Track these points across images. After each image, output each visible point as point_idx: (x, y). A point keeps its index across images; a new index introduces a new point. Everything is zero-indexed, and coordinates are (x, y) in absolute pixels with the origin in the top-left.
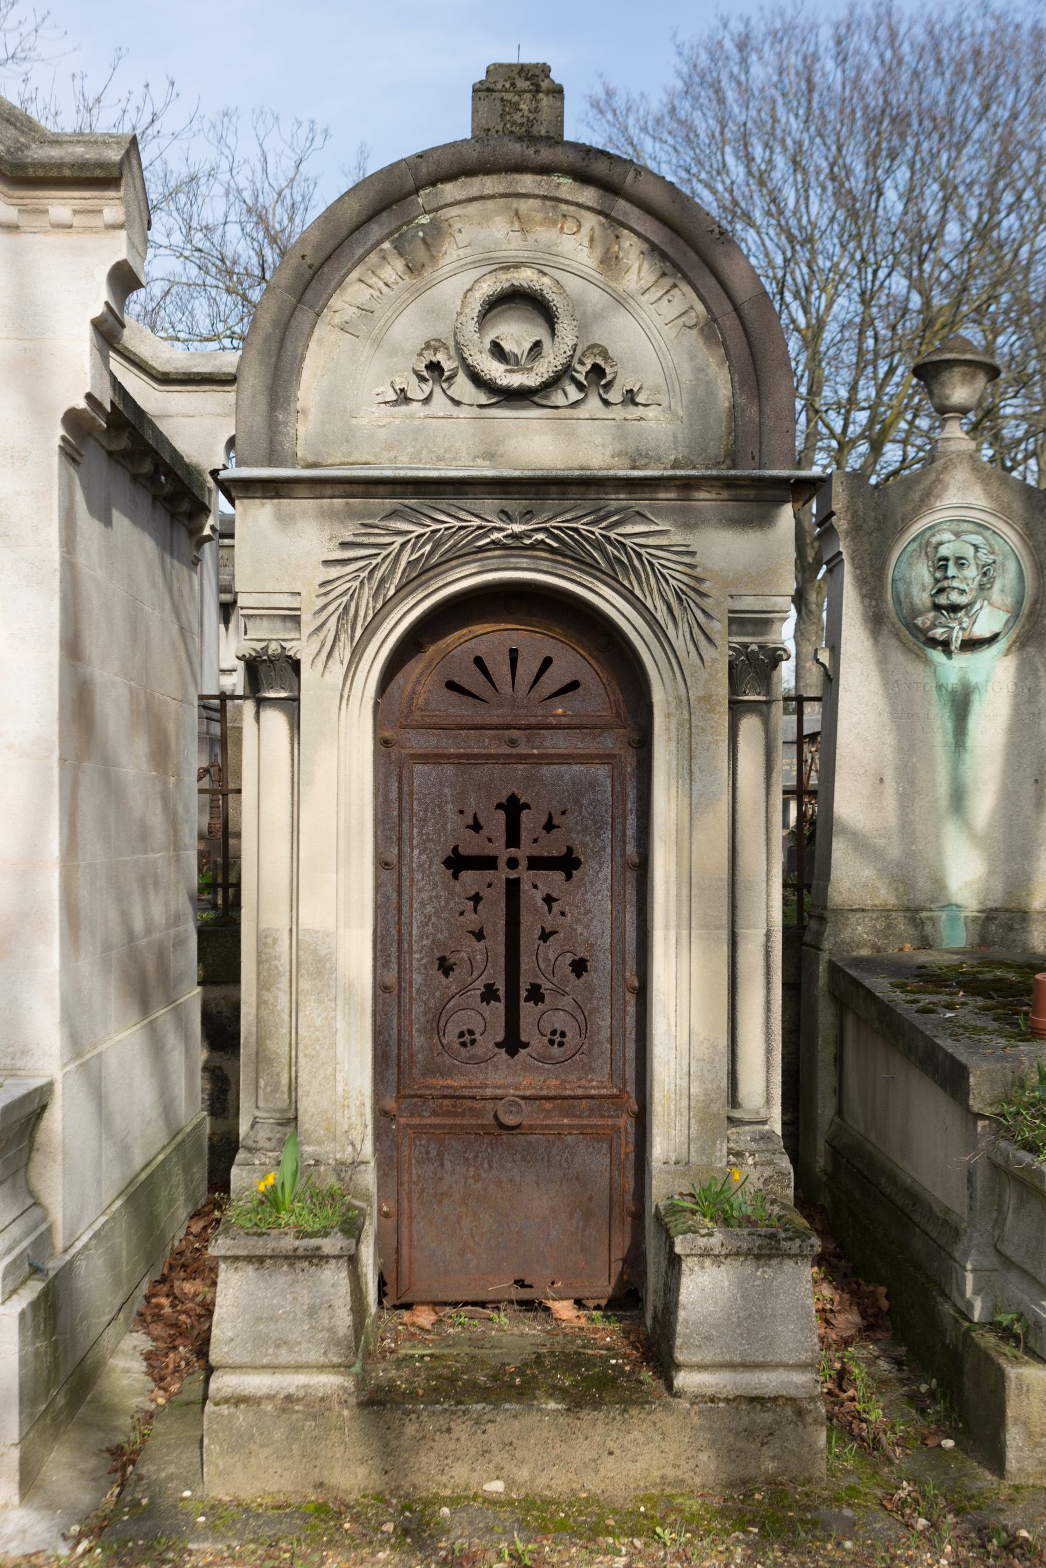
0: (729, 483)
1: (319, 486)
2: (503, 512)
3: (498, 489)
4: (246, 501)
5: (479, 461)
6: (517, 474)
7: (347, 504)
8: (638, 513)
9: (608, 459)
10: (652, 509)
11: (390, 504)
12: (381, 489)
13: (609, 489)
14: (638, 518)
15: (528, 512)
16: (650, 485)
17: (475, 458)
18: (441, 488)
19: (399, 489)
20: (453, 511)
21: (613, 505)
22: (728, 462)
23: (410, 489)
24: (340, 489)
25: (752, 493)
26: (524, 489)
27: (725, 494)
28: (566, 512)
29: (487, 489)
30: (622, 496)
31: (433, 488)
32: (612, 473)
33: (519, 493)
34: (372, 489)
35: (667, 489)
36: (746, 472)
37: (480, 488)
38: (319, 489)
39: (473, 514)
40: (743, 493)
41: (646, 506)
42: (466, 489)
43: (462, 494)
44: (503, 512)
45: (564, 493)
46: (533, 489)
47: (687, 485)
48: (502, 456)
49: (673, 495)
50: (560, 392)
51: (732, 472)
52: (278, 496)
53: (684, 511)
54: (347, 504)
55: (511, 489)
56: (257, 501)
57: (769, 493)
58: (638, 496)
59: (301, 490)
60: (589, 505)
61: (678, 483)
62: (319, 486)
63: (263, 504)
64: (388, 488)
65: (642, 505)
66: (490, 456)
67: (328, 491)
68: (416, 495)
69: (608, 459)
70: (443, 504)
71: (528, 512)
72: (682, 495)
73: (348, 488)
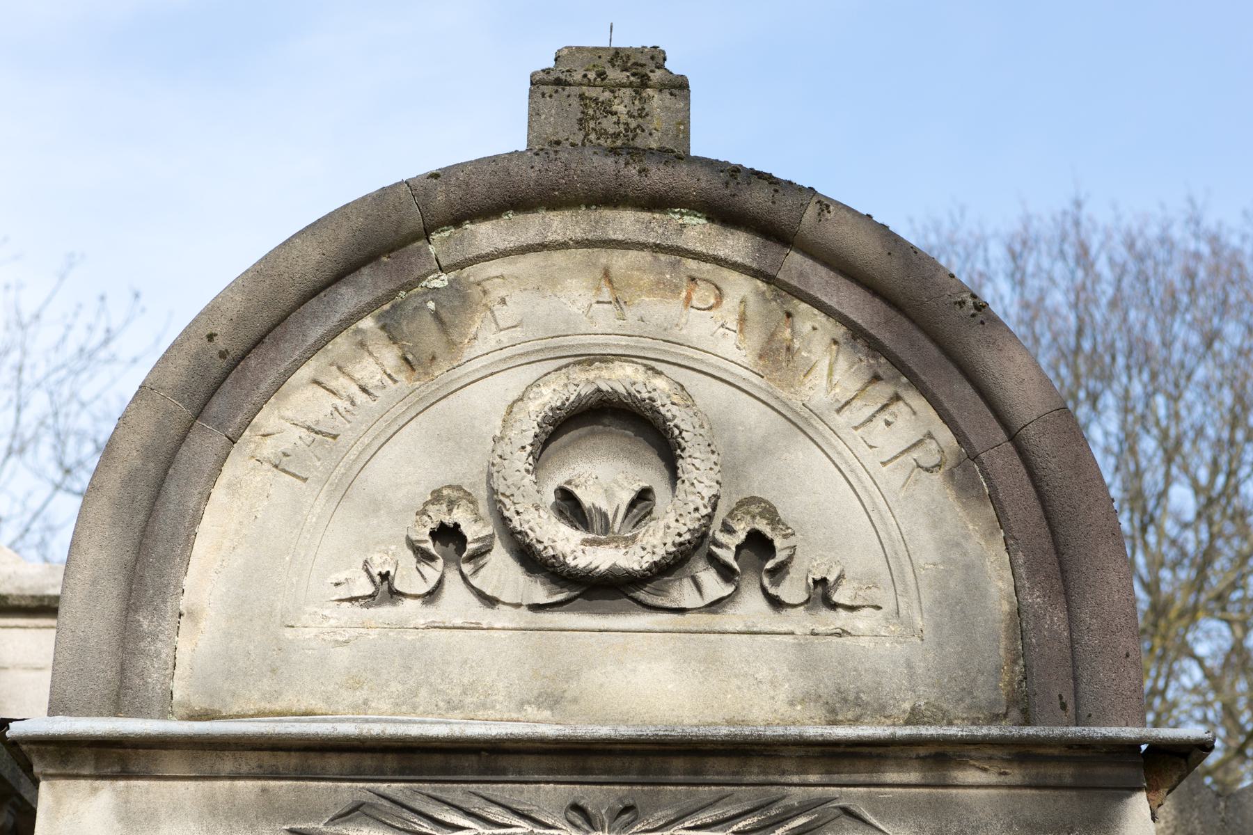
0: (1021, 752)
1: (208, 754)
2: (576, 807)
3: (567, 762)
4: (61, 784)
5: (531, 711)
6: (604, 731)
7: (264, 790)
8: (847, 811)
9: (783, 709)
10: (871, 802)
11: (349, 791)
12: (334, 762)
13: (787, 765)
14: (846, 821)
15: (627, 809)
16: (869, 757)
17: (521, 705)
18: (454, 761)
19: (368, 761)
20: (476, 805)
21: (797, 795)
22: (1015, 713)
23: (391, 761)
24: (250, 761)
25: (1067, 773)
26: (617, 763)
27: (1016, 775)
28: (702, 809)
29: (545, 762)
30: (812, 778)
31: (438, 759)
32: (793, 731)
33: (608, 771)
34: (315, 761)
35: (901, 763)
36: (1057, 731)
37: (530, 761)
38: (209, 761)
39: (515, 812)
40: (1052, 772)
41: (861, 798)
42: (503, 761)
43: (495, 771)
44: (576, 807)
45: (696, 772)
46: (637, 763)
47: (941, 756)
48: (575, 701)
49: (913, 777)
50: (687, 583)
51: (1029, 731)
52: (126, 774)
53: (937, 808)
54: (264, 790)
55: (593, 762)
56: (84, 784)
57: (1103, 772)
58: (844, 778)
59: (173, 762)
60: (747, 796)
61: (922, 751)
62: (208, 754)
63: (95, 790)
64: (348, 760)
65: (853, 796)
66: (551, 701)
67: (228, 766)
68: (402, 774)
69: (783, 709)
70: (456, 792)
71: (627, 809)
72: (932, 777)
73: (267, 758)
